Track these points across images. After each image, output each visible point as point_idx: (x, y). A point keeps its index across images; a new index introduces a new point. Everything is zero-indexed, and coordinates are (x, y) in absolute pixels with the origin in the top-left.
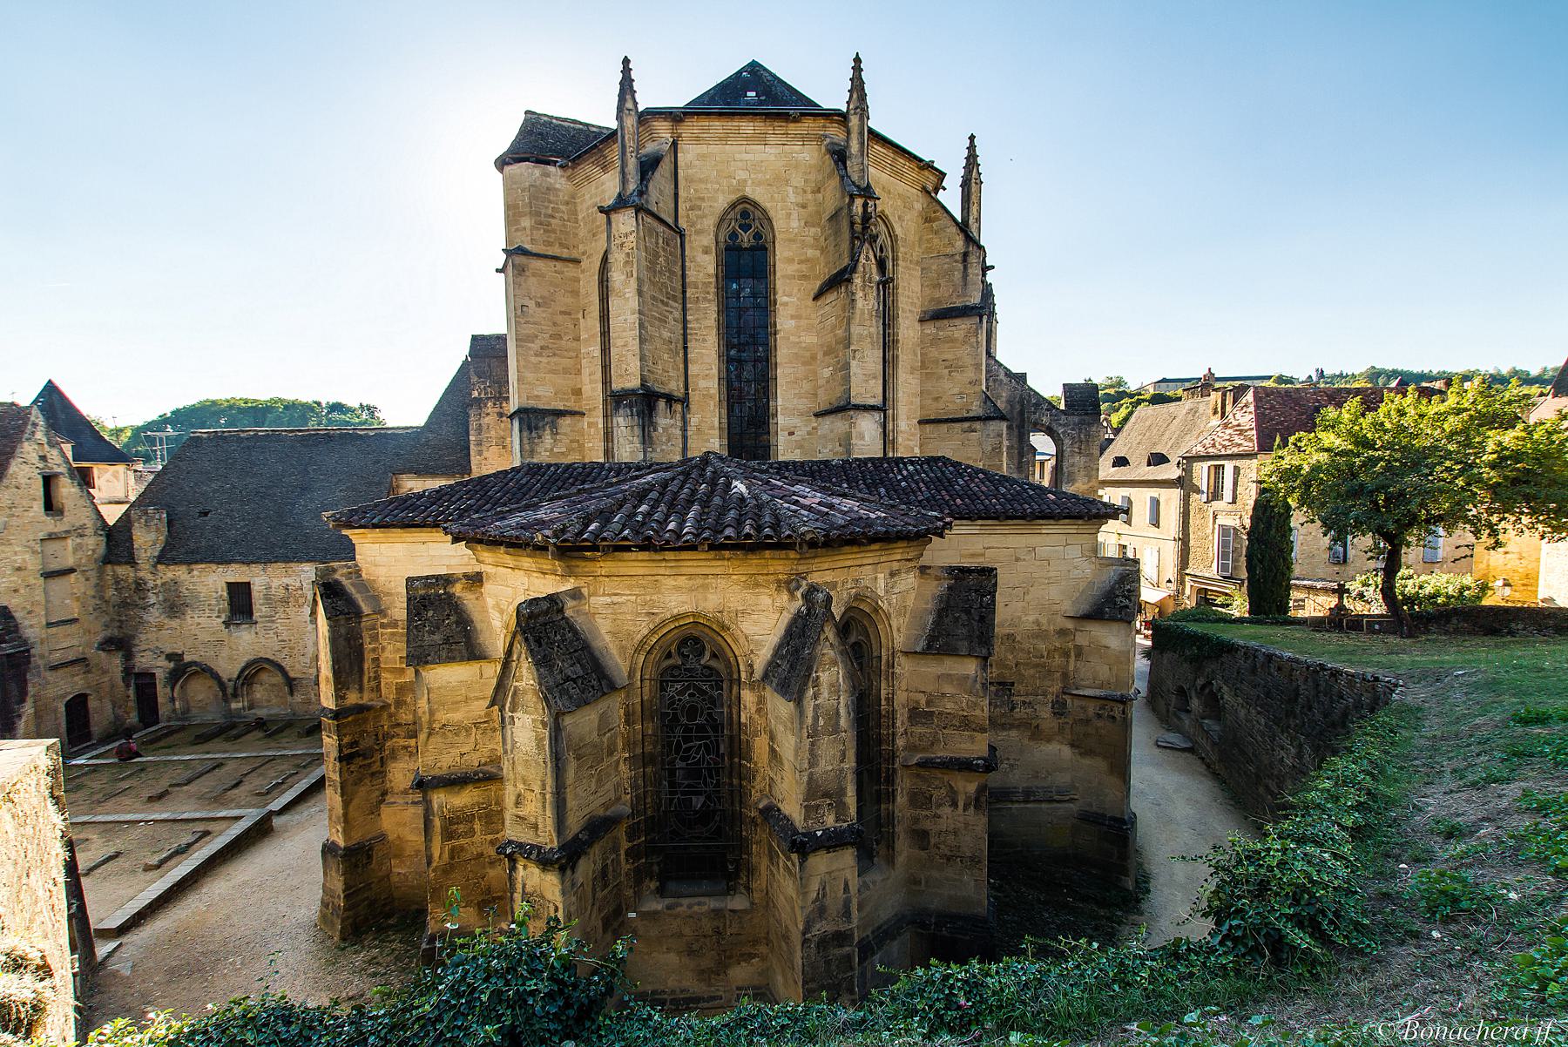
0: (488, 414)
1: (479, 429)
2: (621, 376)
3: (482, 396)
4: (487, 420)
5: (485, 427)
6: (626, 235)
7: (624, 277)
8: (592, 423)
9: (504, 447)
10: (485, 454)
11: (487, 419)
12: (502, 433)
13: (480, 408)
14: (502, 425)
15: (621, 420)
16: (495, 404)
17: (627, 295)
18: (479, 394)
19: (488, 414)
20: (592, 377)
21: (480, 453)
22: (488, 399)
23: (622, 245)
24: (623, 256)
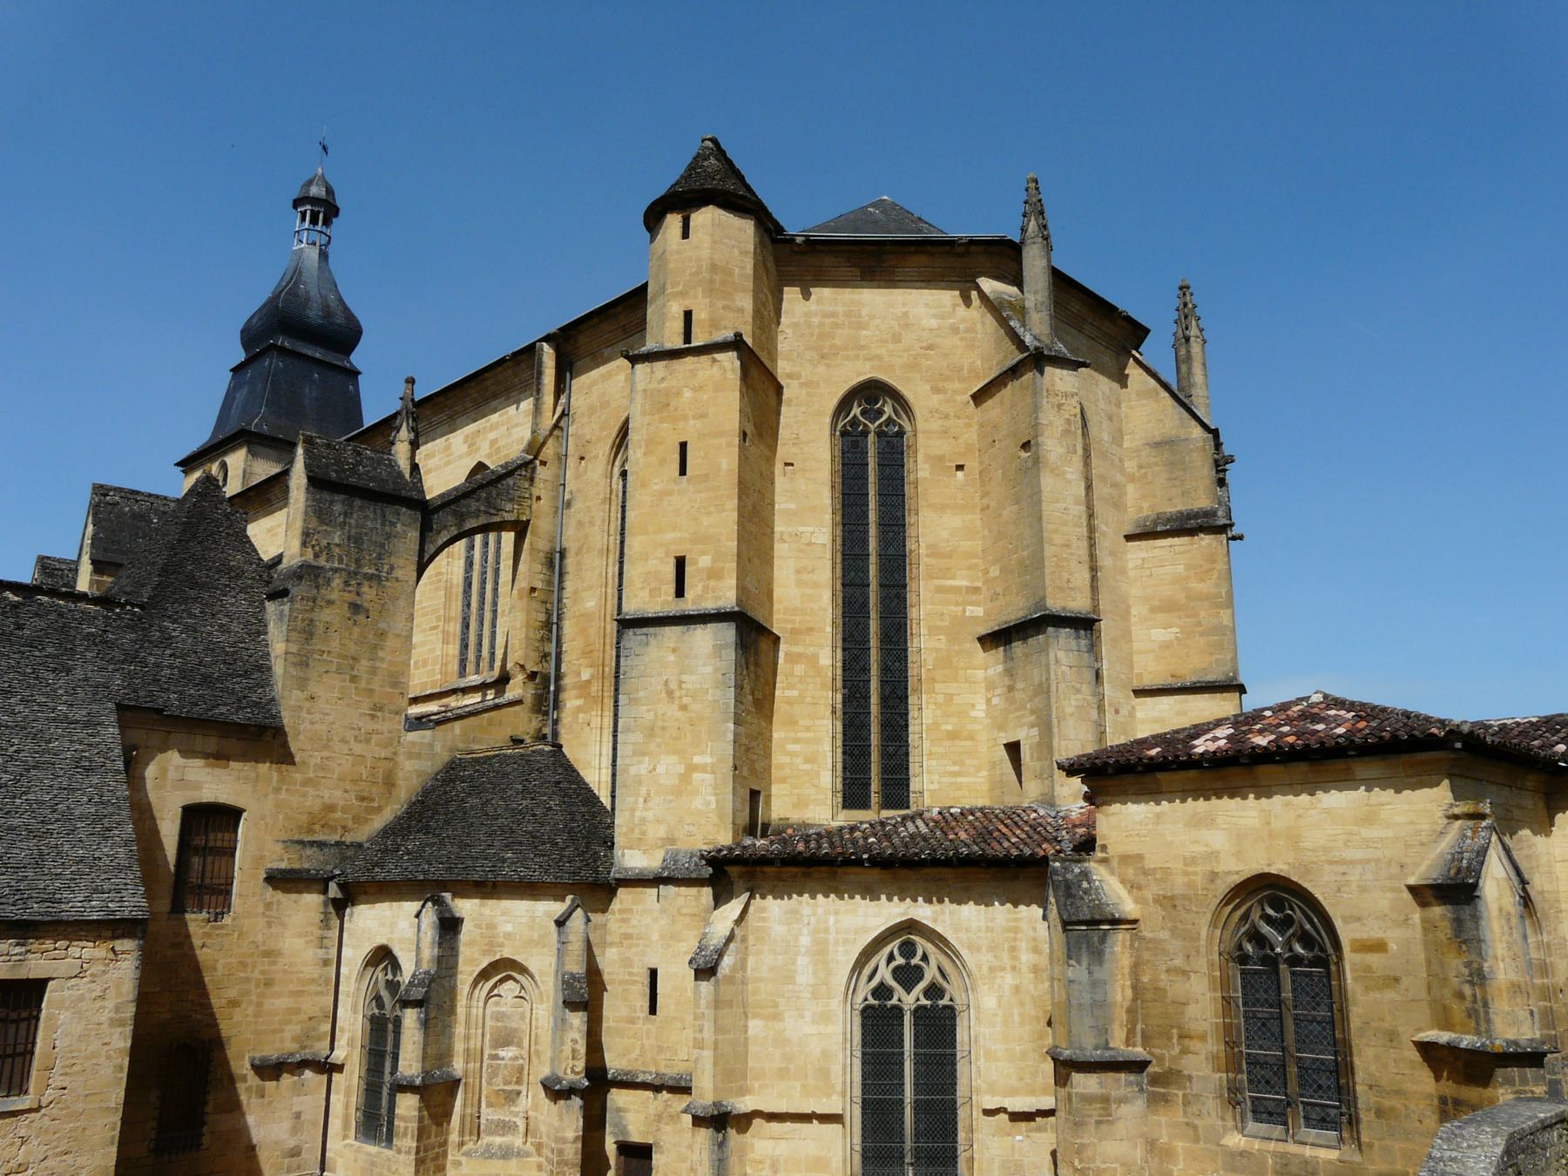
0: (330, 603)
1: (308, 632)
2: (1061, 589)
3: (322, 562)
4: (325, 615)
5: (321, 628)
6: (1066, 395)
7: (1061, 450)
8: (800, 655)
9: (354, 679)
10: (313, 688)
11: (327, 611)
12: (353, 648)
13: (317, 587)
14: (356, 630)
15: (1061, 654)
16: (347, 583)
17: (1069, 476)
18: (316, 556)
19: (330, 603)
20: (805, 577)
21: (302, 683)
22: (335, 570)
23: (1060, 406)
24: (1062, 422)
